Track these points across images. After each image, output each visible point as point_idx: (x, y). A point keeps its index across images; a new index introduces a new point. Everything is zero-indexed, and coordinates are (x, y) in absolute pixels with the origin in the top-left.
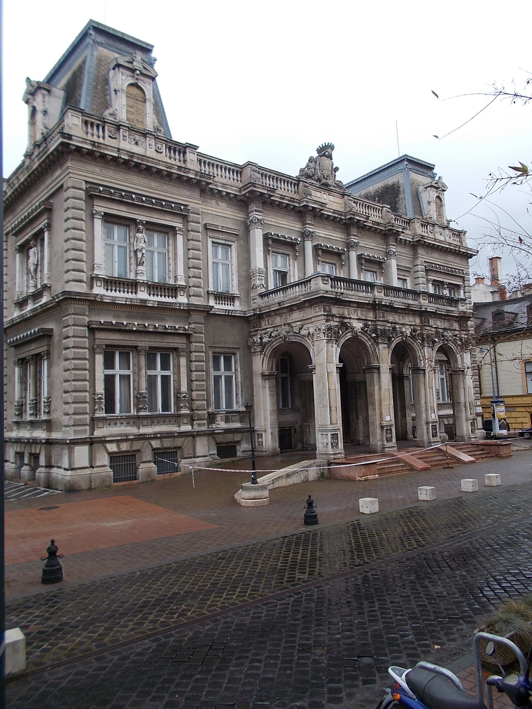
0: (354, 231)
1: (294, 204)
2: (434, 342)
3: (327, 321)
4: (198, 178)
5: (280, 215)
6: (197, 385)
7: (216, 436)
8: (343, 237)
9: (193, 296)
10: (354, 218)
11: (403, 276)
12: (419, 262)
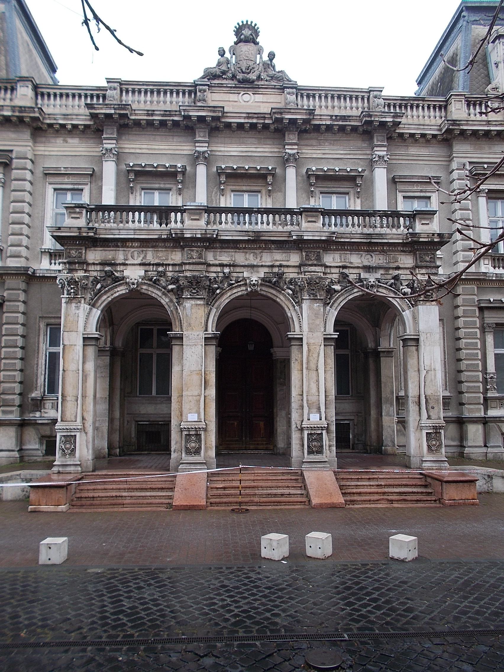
0: (292, 138)
1: (171, 118)
2: (330, 292)
3: (70, 271)
4: (17, 114)
5: (158, 138)
6: (5, 363)
7: (40, 427)
8: (276, 150)
9: (11, 257)
10: (282, 119)
11: (421, 191)
12: (454, 165)
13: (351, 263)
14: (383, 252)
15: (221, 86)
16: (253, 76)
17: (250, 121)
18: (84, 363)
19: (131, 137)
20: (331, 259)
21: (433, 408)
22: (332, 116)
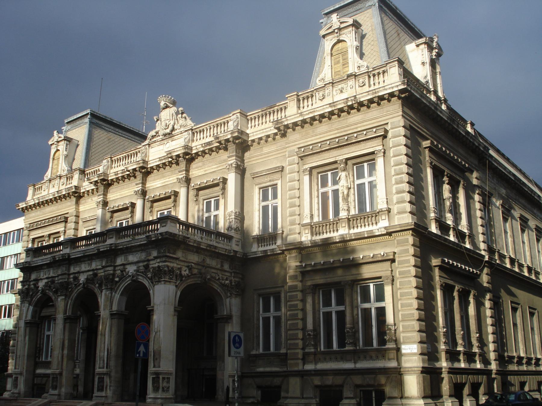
11: (270, 181)
13: (129, 261)
14: (142, 250)
15: (155, 142)
16: (168, 131)
17: (162, 162)
18: (25, 337)
19: (114, 190)
20: (120, 261)
21: (157, 359)
22: (202, 145)
